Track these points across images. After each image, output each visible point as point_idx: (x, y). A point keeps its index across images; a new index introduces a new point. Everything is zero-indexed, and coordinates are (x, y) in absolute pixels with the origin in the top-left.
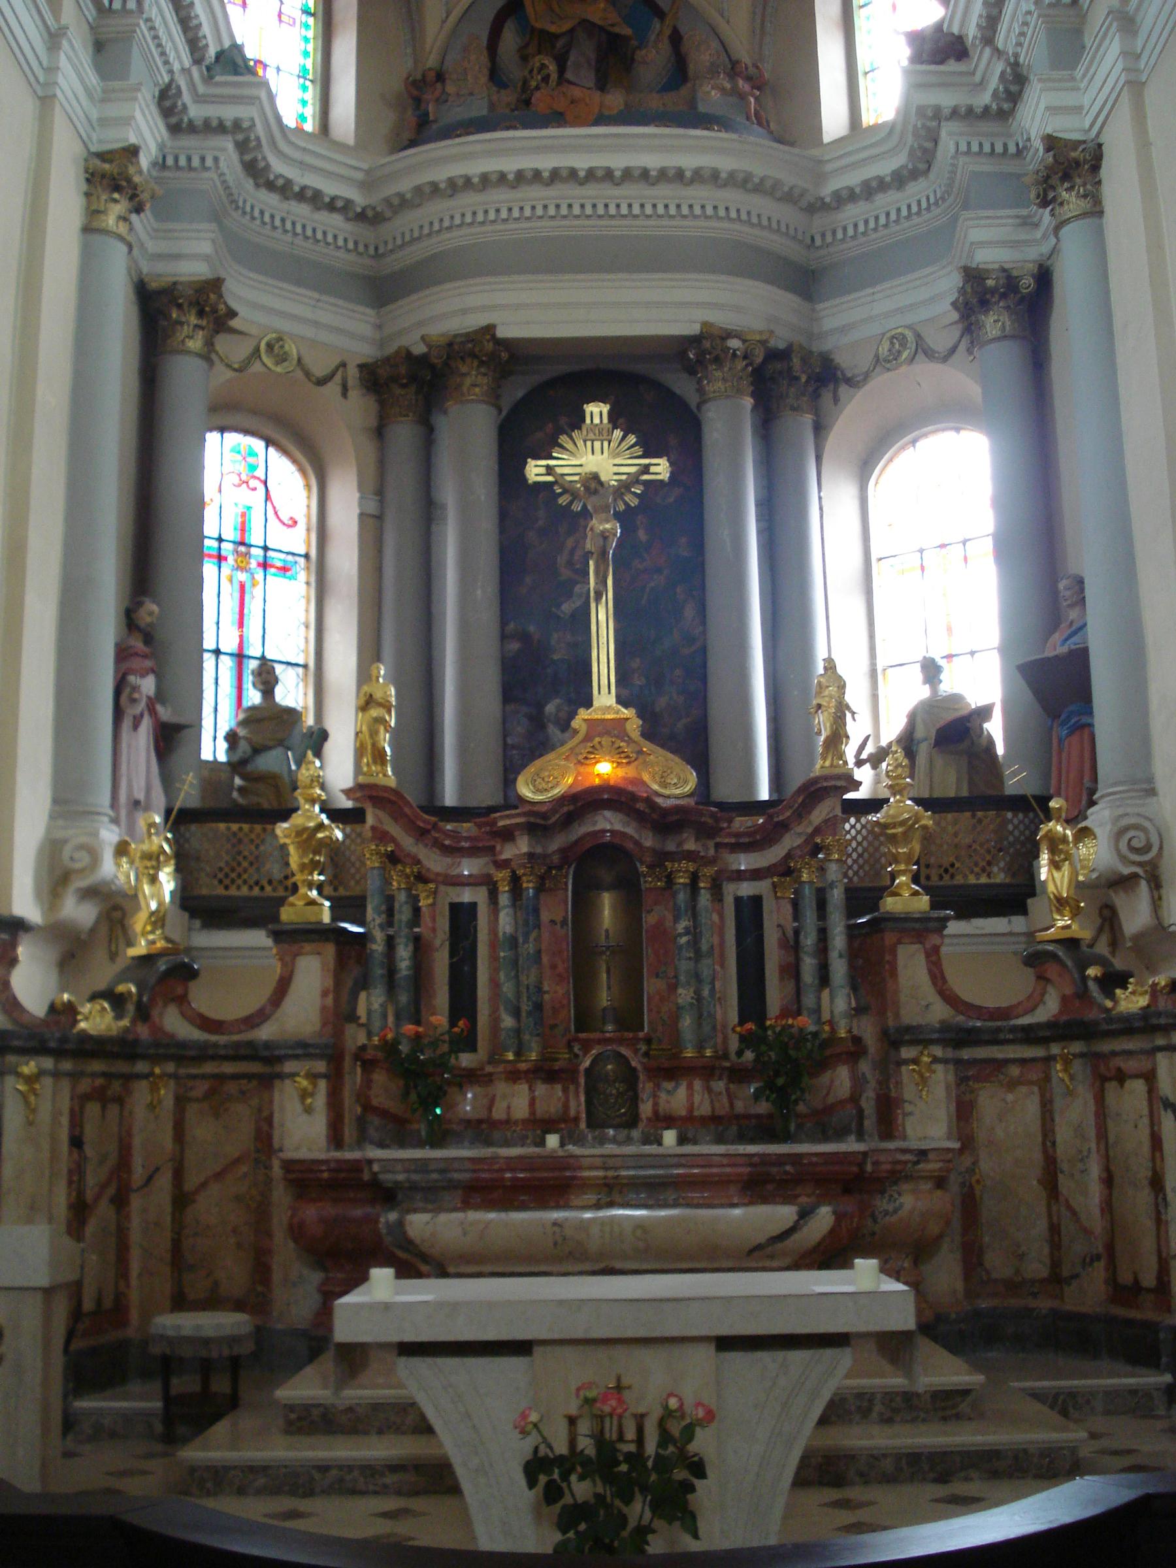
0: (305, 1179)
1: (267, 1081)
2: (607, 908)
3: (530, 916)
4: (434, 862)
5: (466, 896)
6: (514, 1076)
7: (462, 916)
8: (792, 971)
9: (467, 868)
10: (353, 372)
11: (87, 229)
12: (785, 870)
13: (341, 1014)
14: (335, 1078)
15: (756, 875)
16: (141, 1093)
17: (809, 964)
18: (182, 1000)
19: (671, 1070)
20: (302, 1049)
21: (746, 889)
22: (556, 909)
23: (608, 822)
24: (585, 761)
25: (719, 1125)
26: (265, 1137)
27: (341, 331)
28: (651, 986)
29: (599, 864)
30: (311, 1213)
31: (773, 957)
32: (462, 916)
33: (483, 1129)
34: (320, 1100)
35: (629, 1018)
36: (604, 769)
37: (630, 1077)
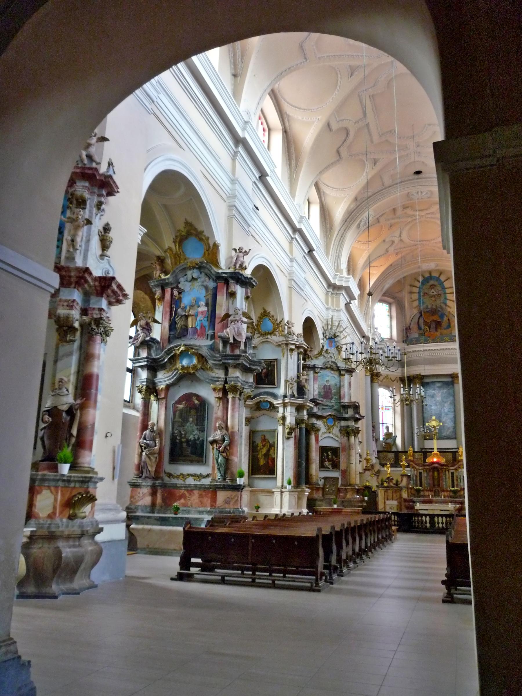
0: (406, 501)
1: (401, 490)
2: (436, 474)
3: (428, 474)
4: (417, 467)
5: (421, 471)
6: (427, 491)
7: (421, 473)
8: (457, 480)
9: (421, 468)
10: (398, 378)
11: (366, 375)
12: (456, 469)
13: (408, 484)
14: (408, 490)
15: (453, 469)
16: (389, 491)
17: (459, 480)
18: (392, 482)
19: (443, 491)
20: (405, 487)
21: (452, 471)
22: (431, 473)
23: (436, 465)
24: (433, 458)
25: (448, 496)
26: (401, 495)
27: (396, 372)
28: (441, 482)
29: (435, 469)
30: (407, 504)
31: (455, 479)
32: (421, 473)
33: (423, 496)
34: (406, 493)
35: (439, 485)
36: (435, 460)
37: (439, 491)
